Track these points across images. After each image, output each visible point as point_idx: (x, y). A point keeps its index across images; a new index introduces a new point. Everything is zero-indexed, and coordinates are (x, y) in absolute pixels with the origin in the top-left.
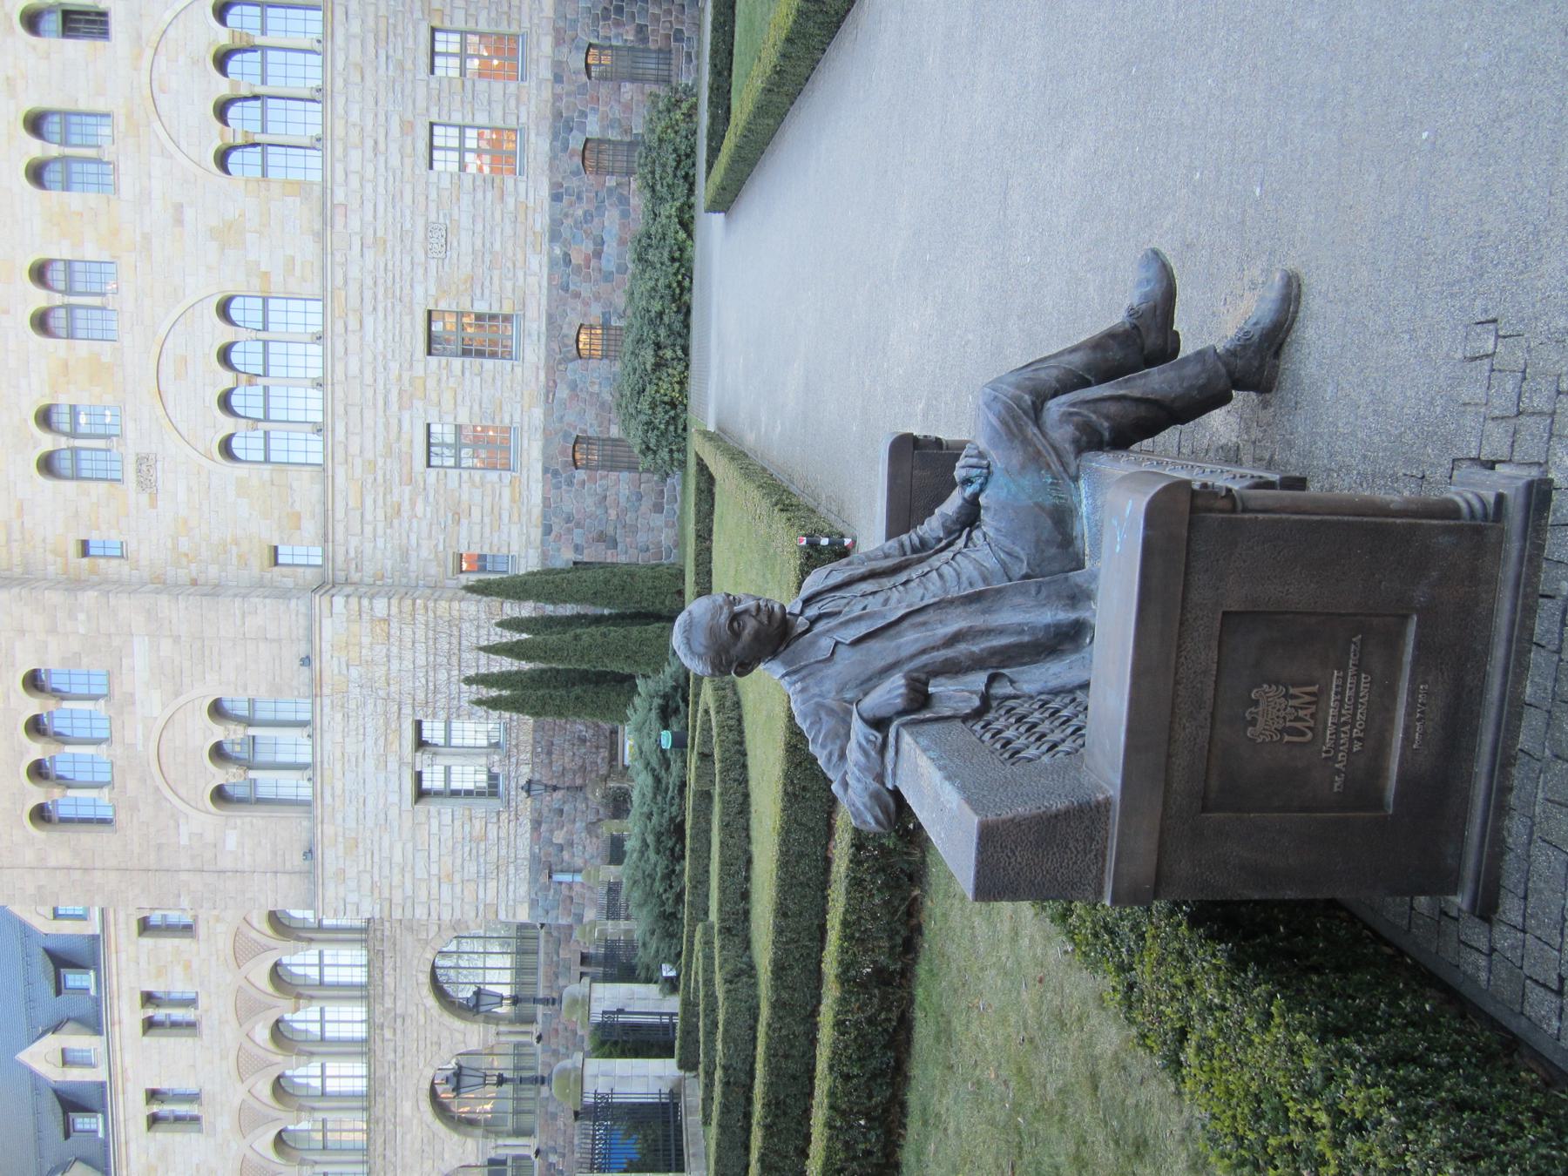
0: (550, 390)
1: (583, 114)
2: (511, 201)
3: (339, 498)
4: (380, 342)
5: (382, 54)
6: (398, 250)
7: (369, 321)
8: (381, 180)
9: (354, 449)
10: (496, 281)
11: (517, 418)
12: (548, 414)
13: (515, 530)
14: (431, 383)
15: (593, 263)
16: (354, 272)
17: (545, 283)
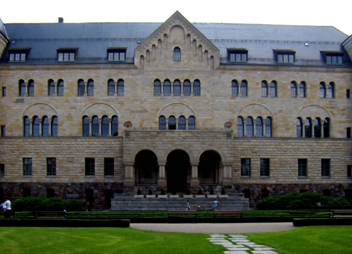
0: (40, 183)
1: (98, 189)
2: (79, 174)
3: (15, 140)
4: (49, 148)
5: (108, 148)
6: (68, 152)
7: (53, 146)
8: (82, 148)
9: (26, 143)
10: (63, 172)
11: (34, 177)
12: (35, 183)
13: (10, 177)
14: (40, 159)
15: (67, 192)
16: (63, 143)
17: (63, 182)
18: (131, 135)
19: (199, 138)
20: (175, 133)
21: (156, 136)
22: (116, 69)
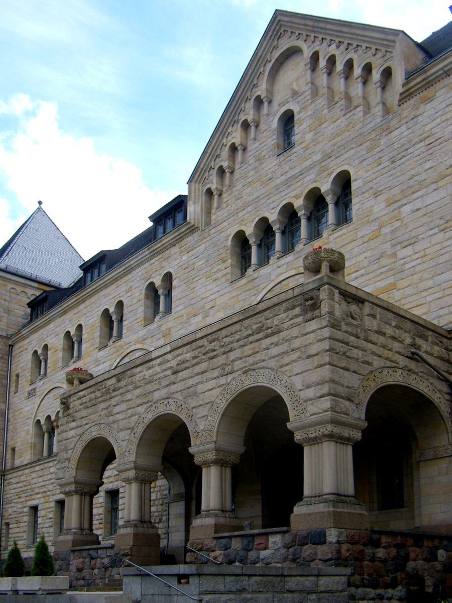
18: (71, 406)
19: (215, 353)
20: (154, 362)
21: (114, 391)
22: (159, 253)
